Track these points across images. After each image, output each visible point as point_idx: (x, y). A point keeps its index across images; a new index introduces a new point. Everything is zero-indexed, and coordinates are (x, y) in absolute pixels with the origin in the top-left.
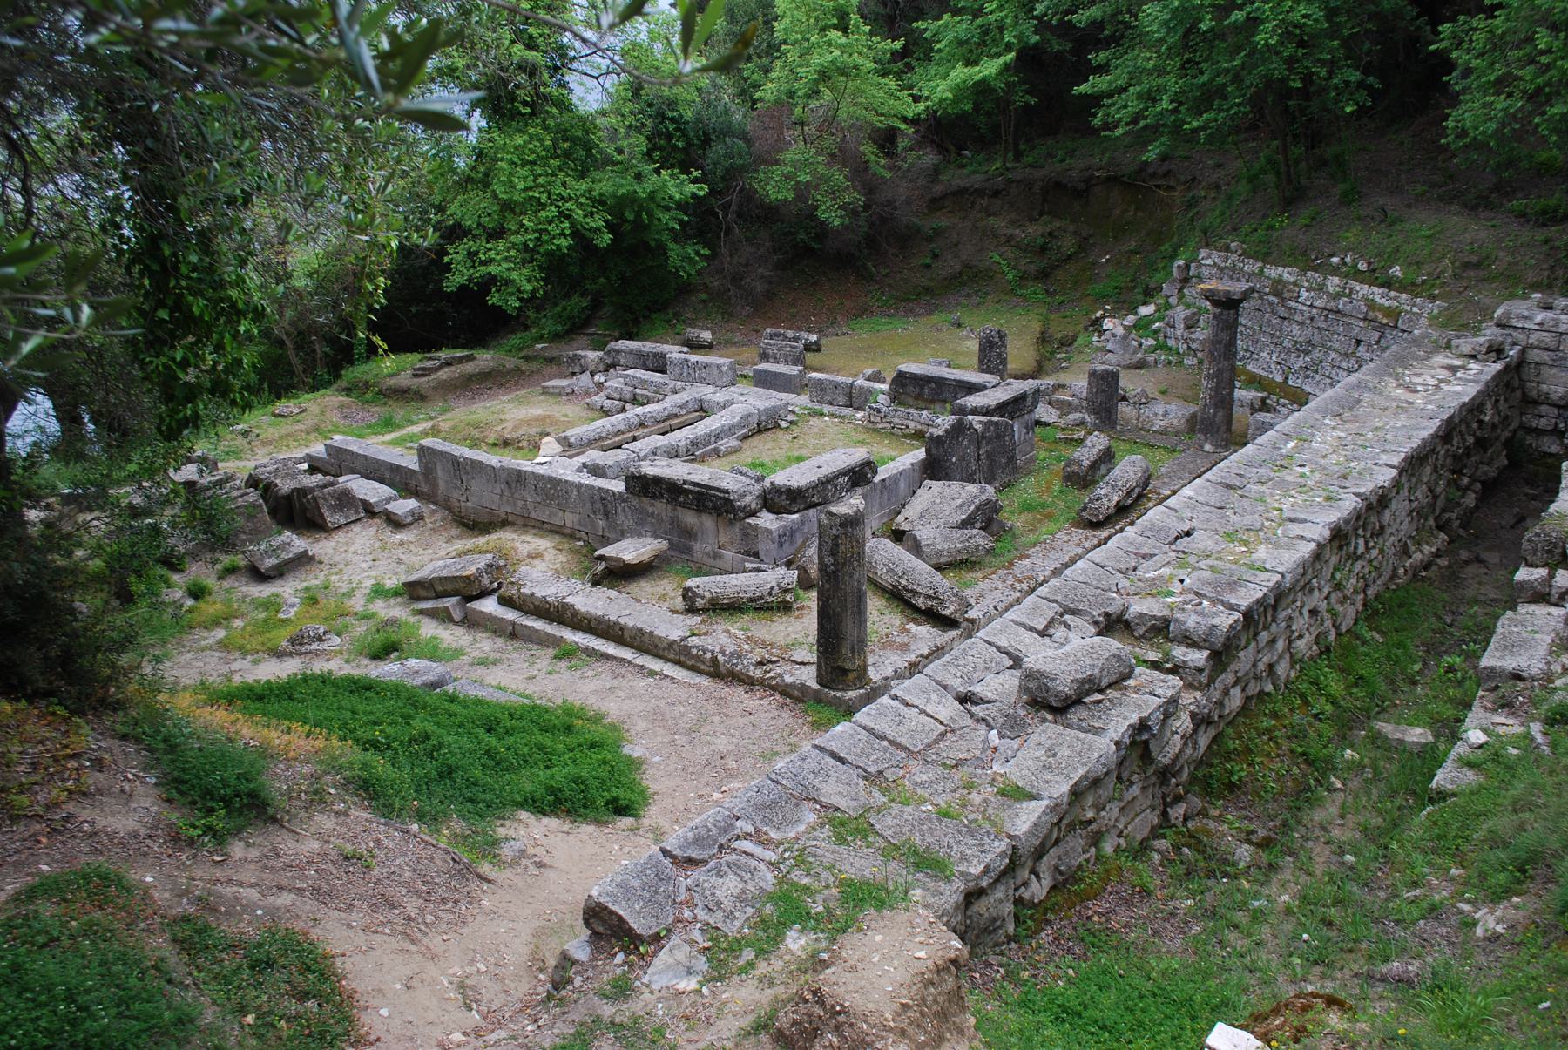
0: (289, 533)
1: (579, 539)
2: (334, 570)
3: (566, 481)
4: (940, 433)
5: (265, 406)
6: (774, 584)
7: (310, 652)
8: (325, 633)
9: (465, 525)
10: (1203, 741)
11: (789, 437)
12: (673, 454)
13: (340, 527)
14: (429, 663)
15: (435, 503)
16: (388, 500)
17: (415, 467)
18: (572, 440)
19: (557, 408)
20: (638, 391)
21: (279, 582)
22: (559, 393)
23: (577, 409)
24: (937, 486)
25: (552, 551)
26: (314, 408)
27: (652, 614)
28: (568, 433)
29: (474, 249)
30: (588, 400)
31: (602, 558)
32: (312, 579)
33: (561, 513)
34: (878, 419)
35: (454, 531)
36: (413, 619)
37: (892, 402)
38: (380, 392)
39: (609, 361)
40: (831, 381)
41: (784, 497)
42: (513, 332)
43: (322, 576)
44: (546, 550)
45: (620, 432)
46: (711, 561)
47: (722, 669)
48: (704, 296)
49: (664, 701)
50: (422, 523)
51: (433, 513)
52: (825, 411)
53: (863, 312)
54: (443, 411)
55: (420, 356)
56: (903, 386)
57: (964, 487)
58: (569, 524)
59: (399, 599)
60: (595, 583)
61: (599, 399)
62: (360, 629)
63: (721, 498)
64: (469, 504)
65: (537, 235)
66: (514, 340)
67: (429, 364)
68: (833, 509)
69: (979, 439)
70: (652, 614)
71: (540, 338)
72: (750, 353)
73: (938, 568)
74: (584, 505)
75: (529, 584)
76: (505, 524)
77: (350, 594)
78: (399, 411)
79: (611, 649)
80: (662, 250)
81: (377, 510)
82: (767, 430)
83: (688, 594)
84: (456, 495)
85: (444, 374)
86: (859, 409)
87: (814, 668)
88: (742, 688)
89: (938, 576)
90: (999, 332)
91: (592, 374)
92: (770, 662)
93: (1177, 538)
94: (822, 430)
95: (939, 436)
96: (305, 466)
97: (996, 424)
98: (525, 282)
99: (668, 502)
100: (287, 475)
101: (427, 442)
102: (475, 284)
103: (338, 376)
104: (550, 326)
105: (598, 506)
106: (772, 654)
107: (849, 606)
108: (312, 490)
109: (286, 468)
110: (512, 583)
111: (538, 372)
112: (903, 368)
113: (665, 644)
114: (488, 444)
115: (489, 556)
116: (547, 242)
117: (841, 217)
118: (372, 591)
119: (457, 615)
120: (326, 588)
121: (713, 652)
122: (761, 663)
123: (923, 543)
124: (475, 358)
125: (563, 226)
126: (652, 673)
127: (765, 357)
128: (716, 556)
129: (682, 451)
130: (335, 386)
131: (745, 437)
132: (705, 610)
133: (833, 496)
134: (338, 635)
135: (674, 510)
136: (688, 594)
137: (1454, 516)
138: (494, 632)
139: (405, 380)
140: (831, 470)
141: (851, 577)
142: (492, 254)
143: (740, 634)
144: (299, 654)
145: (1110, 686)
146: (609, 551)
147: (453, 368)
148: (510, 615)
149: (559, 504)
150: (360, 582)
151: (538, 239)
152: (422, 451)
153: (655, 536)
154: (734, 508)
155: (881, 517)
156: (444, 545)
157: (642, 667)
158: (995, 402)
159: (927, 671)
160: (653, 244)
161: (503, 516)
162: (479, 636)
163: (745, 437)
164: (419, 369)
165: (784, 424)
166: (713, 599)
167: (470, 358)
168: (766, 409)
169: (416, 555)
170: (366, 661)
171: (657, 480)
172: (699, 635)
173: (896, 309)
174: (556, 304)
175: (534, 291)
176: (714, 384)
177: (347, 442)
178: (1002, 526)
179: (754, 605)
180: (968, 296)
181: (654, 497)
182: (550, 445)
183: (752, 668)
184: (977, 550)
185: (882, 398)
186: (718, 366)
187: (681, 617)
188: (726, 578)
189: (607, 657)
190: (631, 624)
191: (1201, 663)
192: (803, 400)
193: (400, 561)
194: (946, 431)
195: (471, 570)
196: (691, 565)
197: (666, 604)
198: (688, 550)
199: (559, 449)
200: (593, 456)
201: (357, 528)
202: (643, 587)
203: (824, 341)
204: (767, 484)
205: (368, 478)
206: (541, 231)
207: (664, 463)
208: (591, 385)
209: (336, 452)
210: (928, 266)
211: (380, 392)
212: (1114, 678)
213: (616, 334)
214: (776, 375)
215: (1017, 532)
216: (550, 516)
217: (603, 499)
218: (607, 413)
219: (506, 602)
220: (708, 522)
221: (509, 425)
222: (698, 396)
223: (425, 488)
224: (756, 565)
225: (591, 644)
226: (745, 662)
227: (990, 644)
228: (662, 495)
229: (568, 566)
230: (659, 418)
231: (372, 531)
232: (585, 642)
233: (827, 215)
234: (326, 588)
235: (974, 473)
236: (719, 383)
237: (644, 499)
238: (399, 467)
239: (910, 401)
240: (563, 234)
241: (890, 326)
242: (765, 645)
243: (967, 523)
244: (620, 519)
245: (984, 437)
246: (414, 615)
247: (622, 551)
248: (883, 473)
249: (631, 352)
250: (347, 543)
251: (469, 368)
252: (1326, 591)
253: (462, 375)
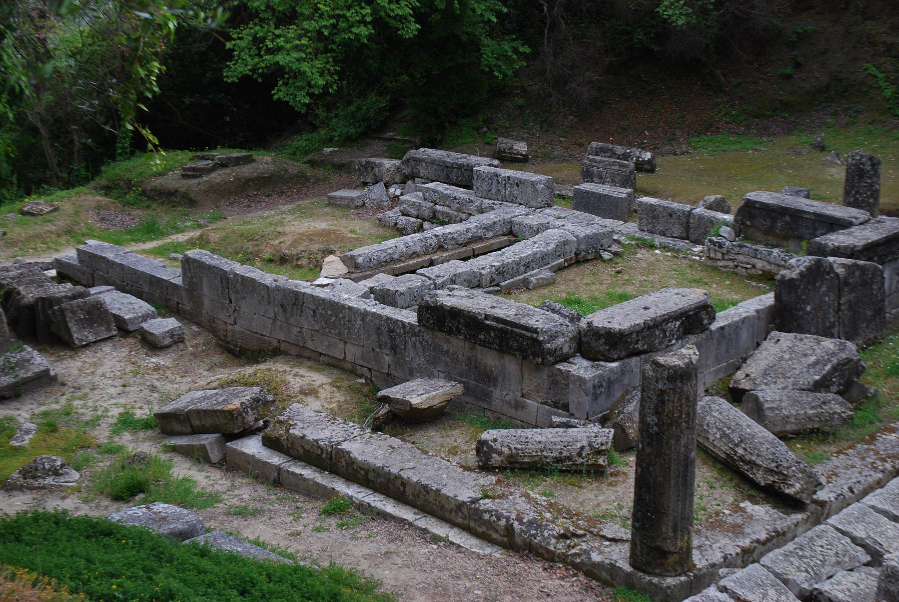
0: (30, 349)
1: (361, 376)
2: (79, 394)
3: (350, 308)
4: (794, 276)
5: (12, 201)
6: (585, 443)
7: (44, 487)
8: (63, 466)
9: (231, 352)
11: (611, 270)
12: (475, 282)
13: (88, 345)
14: (178, 509)
15: (198, 324)
16: (146, 317)
17: (178, 281)
18: (360, 260)
19: (344, 223)
20: (438, 208)
21: (15, 404)
22: (347, 206)
23: (367, 225)
24: (786, 339)
25: (327, 387)
26: (67, 207)
27: (439, 469)
28: (355, 252)
29: (260, 35)
30: (380, 216)
31: (385, 399)
32: (54, 404)
33: (341, 345)
34: (719, 256)
35: (217, 358)
36: (163, 457)
37: (737, 235)
38: (144, 193)
39: (406, 171)
40: (665, 208)
41: (602, 341)
42: (299, 132)
43: (63, 400)
44: (321, 386)
45: (415, 255)
46: (512, 412)
47: (518, 540)
48: (521, 102)
49: (447, 573)
50: (181, 346)
51: (195, 335)
52: (657, 243)
53: (708, 128)
54: (215, 219)
55: (190, 154)
56: (751, 217)
57: (818, 342)
58: (349, 358)
59: (150, 433)
60: (376, 429)
61: (392, 215)
62: (104, 464)
63: (528, 338)
64: (237, 328)
65: (333, 21)
66: (299, 142)
67: (201, 164)
68: (661, 359)
69: (840, 285)
70: (439, 469)
71: (330, 141)
72: (571, 170)
73: (783, 436)
74: (369, 336)
75: (300, 425)
76: (276, 353)
77: (94, 423)
78: (164, 217)
79: (390, 507)
80: (475, 46)
81: (131, 328)
82: (586, 261)
83: (484, 450)
84: (222, 316)
85: (218, 176)
86: (697, 242)
87: (627, 547)
88: (540, 565)
89: (782, 447)
90: (871, 159)
91: (387, 186)
92: (575, 535)
94: (651, 264)
95: (791, 280)
96: (53, 273)
97: (862, 269)
98: (317, 76)
99: (466, 339)
100: (33, 281)
101: (193, 253)
102: (260, 75)
103: (98, 172)
104: (341, 128)
105: (385, 338)
106: (578, 526)
107: (673, 475)
108: (59, 300)
109: (32, 274)
110: (280, 422)
111: (325, 179)
112: (752, 196)
113: (453, 505)
114: (263, 260)
115: (256, 389)
116: (344, 30)
117: (687, 15)
118: (120, 421)
119: (215, 455)
120: (68, 414)
121: (508, 518)
122: (564, 536)
123: (766, 405)
124: (253, 161)
125: (364, 12)
126: (435, 539)
127: (588, 176)
128: (519, 406)
129: (486, 280)
130: (93, 184)
131: (560, 269)
132: (502, 469)
133: (660, 343)
134: (78, 469)
135: (473, 348)
136: (484, 450)
138: (256, 477)
139: (172, 181)
140: (659, 313)
141: (678, 440)
142: (281, 42)
143: (542, 499)
144: (31, 488)
146: (394, 392)
147: (228, 171)
148: (276, 459)
149: (339, 334)
150: (107, 410)
151: (334, 26)
152: (188, 264)
153: (449, 378)
154: (543, 351)
155: (717, 372)
156: (205, 373)
157: (424, 531)
158: (863, 243)
159: (765, 560)
160: (465, 38)
161: (275, 344)
162: (238, 481)
163: (560, 269)
164: (189, 169)
165: (606, 256)
166: (511, 456)
167: (248, 160)
168: (587, 237)
169: (172, 382)
170: (106, 502)
171: (455, 313)
172: (494, 498)
173: (747, 127)
174: (349, 103)
175: (326, 87)
176: (527, 205)
177: (103, 249)
178: (864, 391)
179: (560, 466)
180: (835, 114)
181: (450, 332)
182: (333, 265)
183: (553, 541)
184: (832, 419)
185: (725, 231)
186: (533, 184)
187: (474, 475)
188: (529, 432)
189: (384, 516)
190: (414, 479)
192: (631, 227)
193: (153, 388)
194: (801, 274)
195: (235, 404)
196: (489, 414)
197: (457, 458)
198: (486, 396)
199: (344, 269)
200: (383, 280)
201: (107, 348)
202: (432, 437)
203: (659, 160)
204: (583, 324)
205: (124, 291)
206: (338, 17)
207: (464, 293)
208: (385, 198)
209: (88, 258)
210: (788, 77)
211: (144, 193)
213: (417, 140)
214: (601, 197)
215: (882, 399)
216: (329, 346)
217: (390, 331)
218: (401, 232)
219: (271, 443)
220: (511, 365)
221: (288, 240)
222: (507, 217)
223: (187, 306)
224: (565, 420)
225: (367, 500)
226: (546, 534)
227: (843, 533)
228: (459, 331)
229: (345, 406)
230: (461, 240)
231: (124, 352)
232: (360, 496)
233: (670, 12)
234: (68, 414)
235: (832, 325)
236: (533, 203)
237: (439, 334)
238: (160, 280)
239: (759, 235)
240: (362, 22)
241: (739, 147)
242: (571, 515)
243: (819, 386)
244: (410, 354)
245: (846, 283)
246: (166, 452)
247: (409, 393)
248: (722, 319)
249: (433, 162)
250: (95, 365)
251: (246, 171)
253: (237, 179)
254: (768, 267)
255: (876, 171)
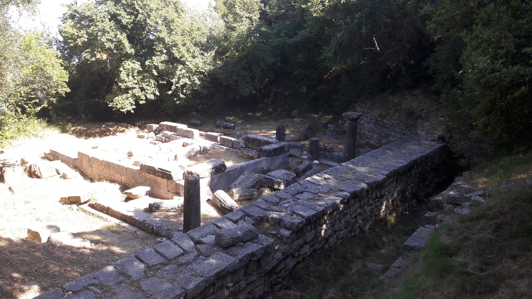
10: (291, 263)
34: (240, 152)
39: (160, 128)
93: (298, 194)
121: (153, 226)
137: (421, 194)
145: (248, 241)
191: (288, 236)
212: (250, 238)
243: (252, 187)
252: (354, 215)
254: (252, 155)
255: (284, 129)
